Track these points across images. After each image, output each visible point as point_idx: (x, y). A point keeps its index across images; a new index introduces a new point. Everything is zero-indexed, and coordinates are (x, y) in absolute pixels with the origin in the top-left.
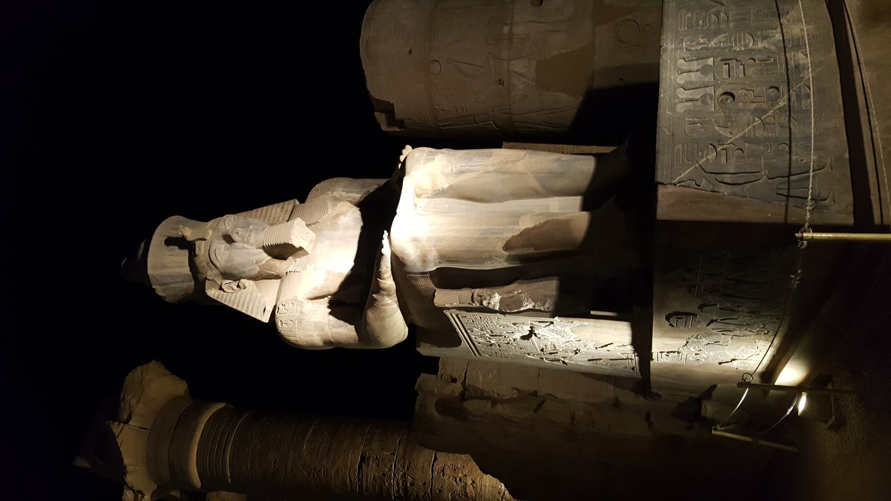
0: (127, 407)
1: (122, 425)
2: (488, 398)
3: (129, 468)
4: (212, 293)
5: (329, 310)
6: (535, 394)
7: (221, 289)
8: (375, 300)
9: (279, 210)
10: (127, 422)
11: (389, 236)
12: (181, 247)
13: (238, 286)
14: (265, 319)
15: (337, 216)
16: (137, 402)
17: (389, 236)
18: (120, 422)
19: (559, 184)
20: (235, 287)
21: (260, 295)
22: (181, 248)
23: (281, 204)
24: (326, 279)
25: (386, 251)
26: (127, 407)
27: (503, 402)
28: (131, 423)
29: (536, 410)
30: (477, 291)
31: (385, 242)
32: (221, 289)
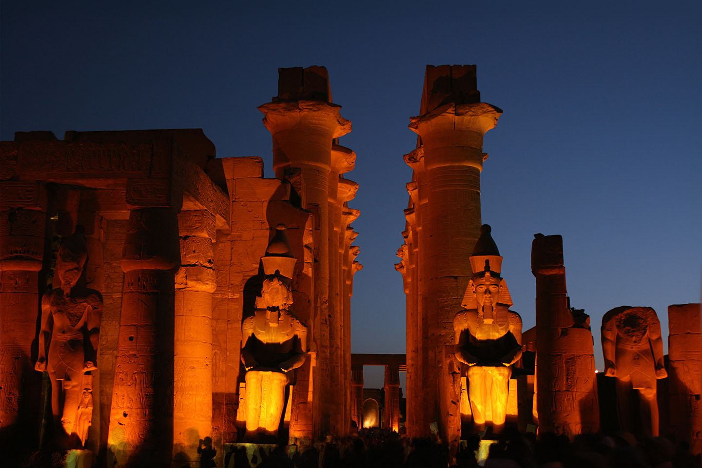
0: (466, 111)
1: (454, 112)
2: (454, 383)
3: (429, 122)
6: (458, 401)
7: (473, 285)
10: (456, 114)
11: (474, 365)
13: (474, 292)
16: (470, 115)
17: (474, 365)
18: (455, 111)
19: (494, 415)
22: (485, 267)
25: (470, 365)
26: (466, 111)
27: (454, 389)
28: (456, 117)
29: (452, 402)
30: (466, 391)
31: (473, 364)
32: (473, 285)
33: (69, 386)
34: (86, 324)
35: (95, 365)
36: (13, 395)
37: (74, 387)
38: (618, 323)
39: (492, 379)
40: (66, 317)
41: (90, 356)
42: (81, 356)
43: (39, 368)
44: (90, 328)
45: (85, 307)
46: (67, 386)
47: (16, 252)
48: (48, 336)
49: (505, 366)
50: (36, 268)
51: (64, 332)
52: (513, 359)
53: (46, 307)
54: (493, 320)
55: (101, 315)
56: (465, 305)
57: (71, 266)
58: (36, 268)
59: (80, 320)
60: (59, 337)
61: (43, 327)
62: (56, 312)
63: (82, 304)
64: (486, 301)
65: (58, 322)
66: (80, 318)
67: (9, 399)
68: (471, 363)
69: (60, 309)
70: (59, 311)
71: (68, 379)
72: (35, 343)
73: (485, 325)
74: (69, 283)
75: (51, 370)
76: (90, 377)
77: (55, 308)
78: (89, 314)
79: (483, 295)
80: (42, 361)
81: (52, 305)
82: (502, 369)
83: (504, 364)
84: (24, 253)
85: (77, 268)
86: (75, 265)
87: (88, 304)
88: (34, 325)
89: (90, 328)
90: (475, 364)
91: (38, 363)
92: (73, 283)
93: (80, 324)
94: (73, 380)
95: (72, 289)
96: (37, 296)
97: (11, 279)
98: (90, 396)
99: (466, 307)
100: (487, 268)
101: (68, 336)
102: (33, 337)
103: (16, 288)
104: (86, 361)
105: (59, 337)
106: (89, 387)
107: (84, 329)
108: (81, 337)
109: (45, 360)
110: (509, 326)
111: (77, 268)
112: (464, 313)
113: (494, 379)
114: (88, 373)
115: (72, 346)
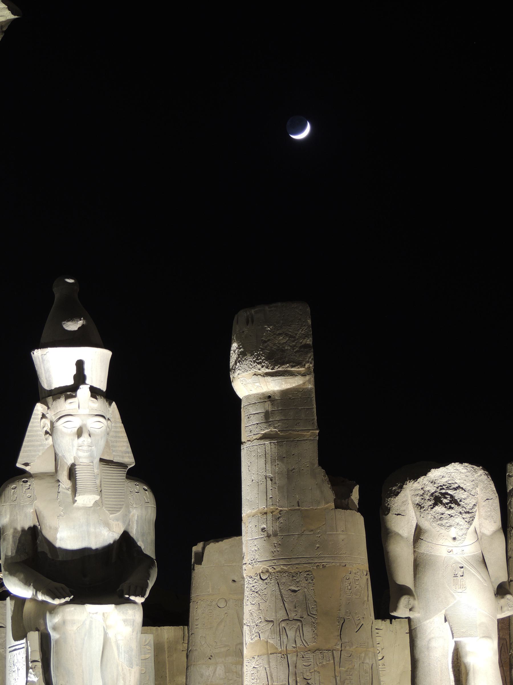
4: (39, 408)
5: (26, 529)
7: (44, 416)
8: (30, 585)
9: (124, 449)
11: (67, 603)
12: (76, 377)
13: (47, 433)
14: (18, 465)
15: (107, 525)
17: (67, 603)
20: (45, 429)
21: (40, 454)
23: (130, 449)
24: (50, 528)
25: (57, 602)
30: (39, 665)
31: (63, 601)
32: (44, 416)
38: (418, 499)
39: (106, 634)
49: (134, 602)
52: (147, 586)
54: (97, 497)
56: (27, 464)
64: (81, 454)
68: (59, 598)
73: (79, 509)
79: (73, 440)
82: (127, 608)
83: (132, 598)
90: (68, 599)
99: (27, 468)
100: (80, 377)
110: (129, 512)
112: (27, 481)
113: (111, 635)
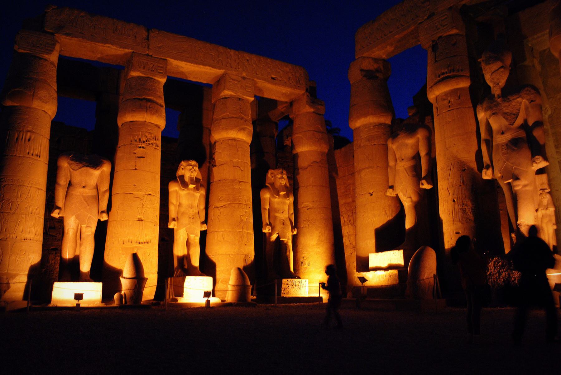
33: (519, 186)
34: (526, 121)
35: (546, 159)
36: (466, 205)
37: (525, 186)
40: (501, 117)
41: (538, 150)
42: (527, 153)
43: (487, 175)
44: (531, 123)
45: (521, 103)
46: (517, 186)
47: (443, 74)
48: (489, 144)
50: (465, 84)
51: (503, 133)
53: (481, 116)
55: (541, 108)
57: (495, 66)
58: (465, 84)
59: (517, 117)
60: (500, 140)
61: (483, 135)
62: (490, 116)
63: (516, 101)
65: (495, 126)
66: (517, 116)
67: (464, 211)
69: (494, 112)
70: (494, 114)
71: (516, 178)
72: (479, 154)
74: (498, 84)
75: (498, 175)
76: (544, 177)
77: (489, 113)
78: (526, 109)
80: (487, 168)
81: (486, 110)
84: (450, 73)
85: (502, 67)
86: (499, 64)
87: (523, 98)
88: (474, 137)
89: (531, 123)
91: (484, 171)
92: (502, 82)
93: (519, 121)
94: (522, 179)
95: (503, 90)
96: (472, 109)
97: (444, 100)
98: (548, 196)
101: (508, 136)
102: (475, 148)
103: (450, 106)
104: (533, 156)
105: (500, 140)
106: (546, 186)
107: (524, 126)
108: (523, 134)
109: (491, 166)
111: (502, 67)
114: (540, 172)
115: (514, 144)
